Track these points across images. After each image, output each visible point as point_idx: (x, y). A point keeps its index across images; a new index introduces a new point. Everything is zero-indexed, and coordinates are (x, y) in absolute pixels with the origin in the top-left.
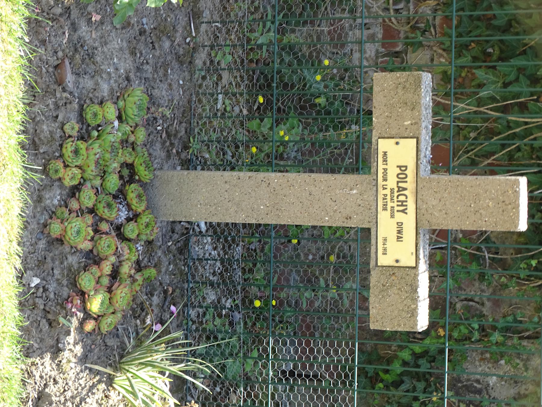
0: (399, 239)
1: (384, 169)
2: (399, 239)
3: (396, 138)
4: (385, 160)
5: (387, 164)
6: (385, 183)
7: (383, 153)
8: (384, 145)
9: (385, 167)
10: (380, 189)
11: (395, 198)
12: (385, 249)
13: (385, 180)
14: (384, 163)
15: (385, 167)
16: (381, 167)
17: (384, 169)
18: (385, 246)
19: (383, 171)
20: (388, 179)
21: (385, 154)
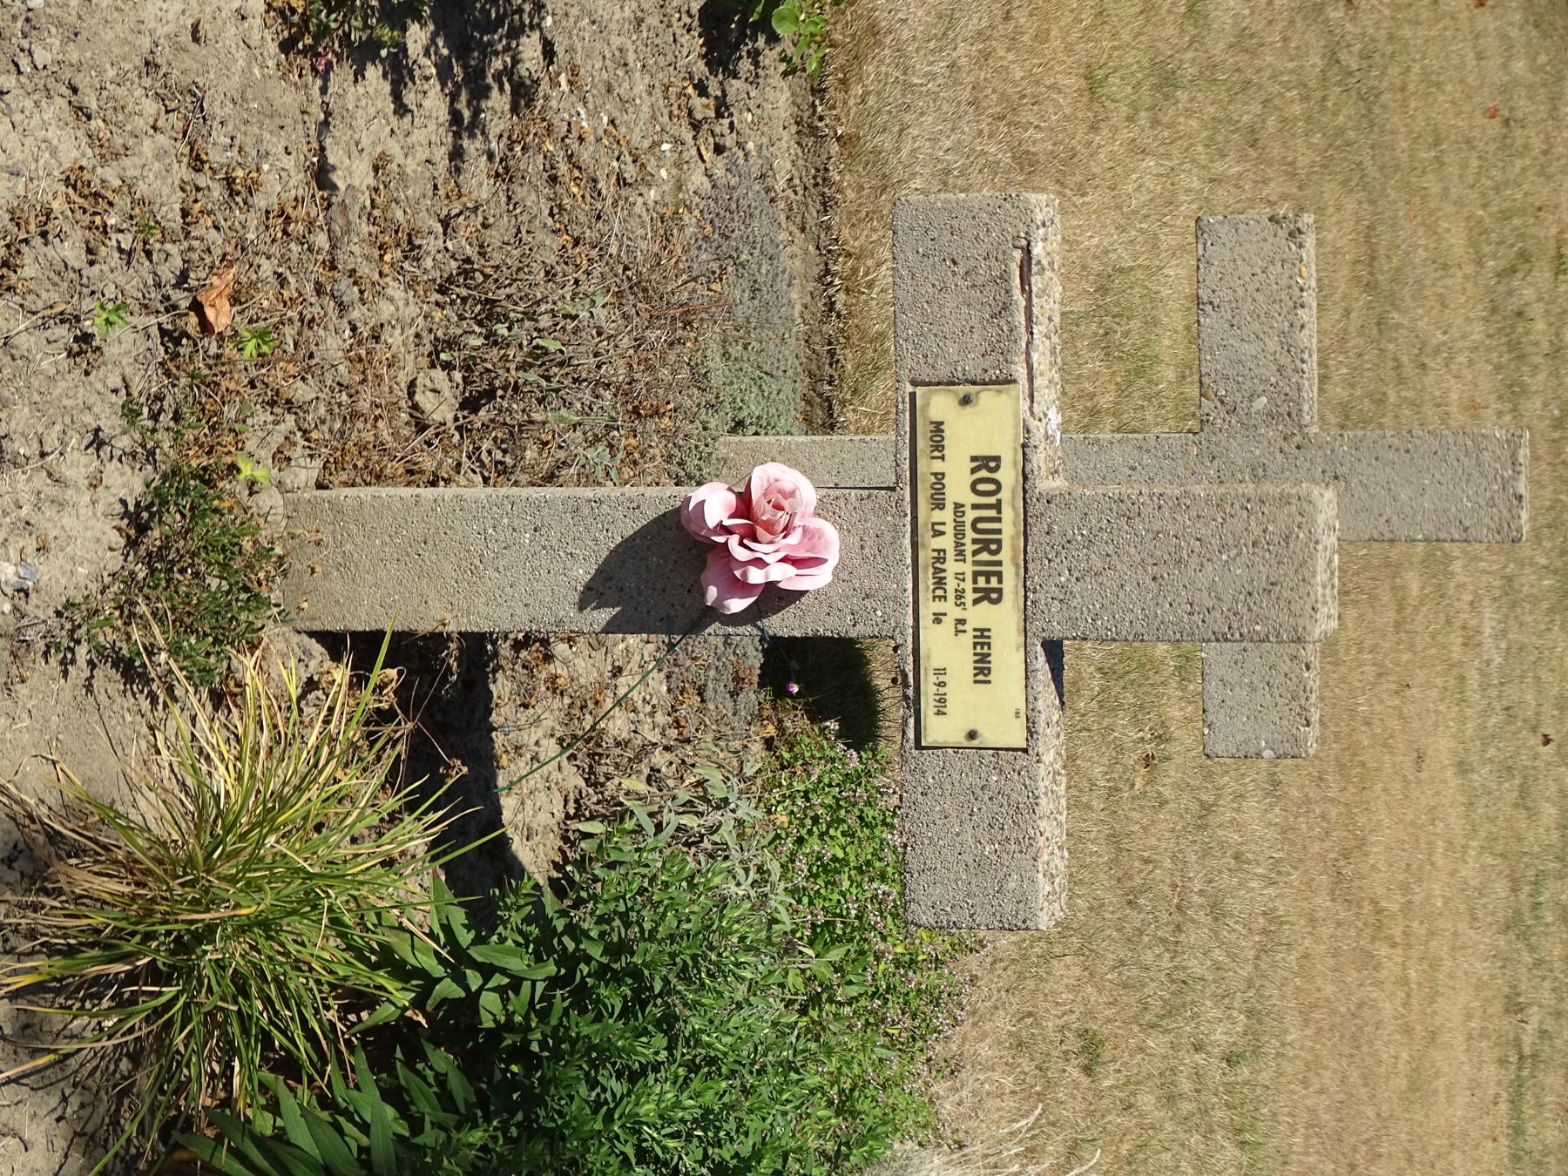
0: (982, 669)
1: (935, 474)
2: (982, 669)
4: (938, 447)
5: (943, 458)
6: (937, 516)
7: (932, 427)
9: (938, 466)
11: (968, 554)
12: (942, 700)
13: (940, 505)
14: (936, 454)
15: (938, 466)
18: (942, 690)
21: (938, 427)
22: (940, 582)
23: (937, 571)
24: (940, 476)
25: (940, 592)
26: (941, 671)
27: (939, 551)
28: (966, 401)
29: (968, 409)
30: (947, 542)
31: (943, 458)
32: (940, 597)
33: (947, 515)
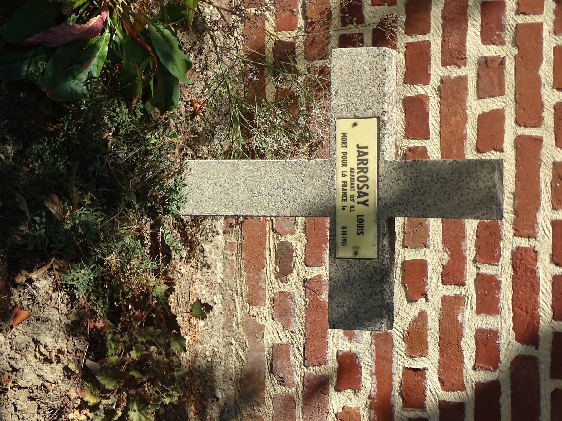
1: (343, 153)
3: (356, 117)
4: (344, 142)
5: (346, 147)
6: (344, 169)
7: (342, 135)
8: (343, 126)
9: (344, 150)
10: (339, 174)
13: (344, 164)
14: (344, 145)
15: (344, 150)
16: (340, 150)
17: (343, 153)
18: (345, 236)
19: (342, 155)
20: (348, 164)
21: (344, 135)
22: (344, 194)
23: (343, 190)
24: (345, 154)
25: (344, 198)
26: (344, 228)
27: (344, 182)
28: (355, 124)
29: (355, 127)
30: (347, 179)
31: (346, 147)
32: (344, 200)
33: (347, 169)
